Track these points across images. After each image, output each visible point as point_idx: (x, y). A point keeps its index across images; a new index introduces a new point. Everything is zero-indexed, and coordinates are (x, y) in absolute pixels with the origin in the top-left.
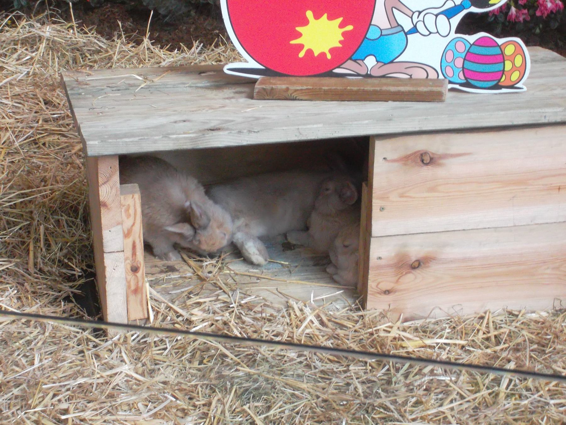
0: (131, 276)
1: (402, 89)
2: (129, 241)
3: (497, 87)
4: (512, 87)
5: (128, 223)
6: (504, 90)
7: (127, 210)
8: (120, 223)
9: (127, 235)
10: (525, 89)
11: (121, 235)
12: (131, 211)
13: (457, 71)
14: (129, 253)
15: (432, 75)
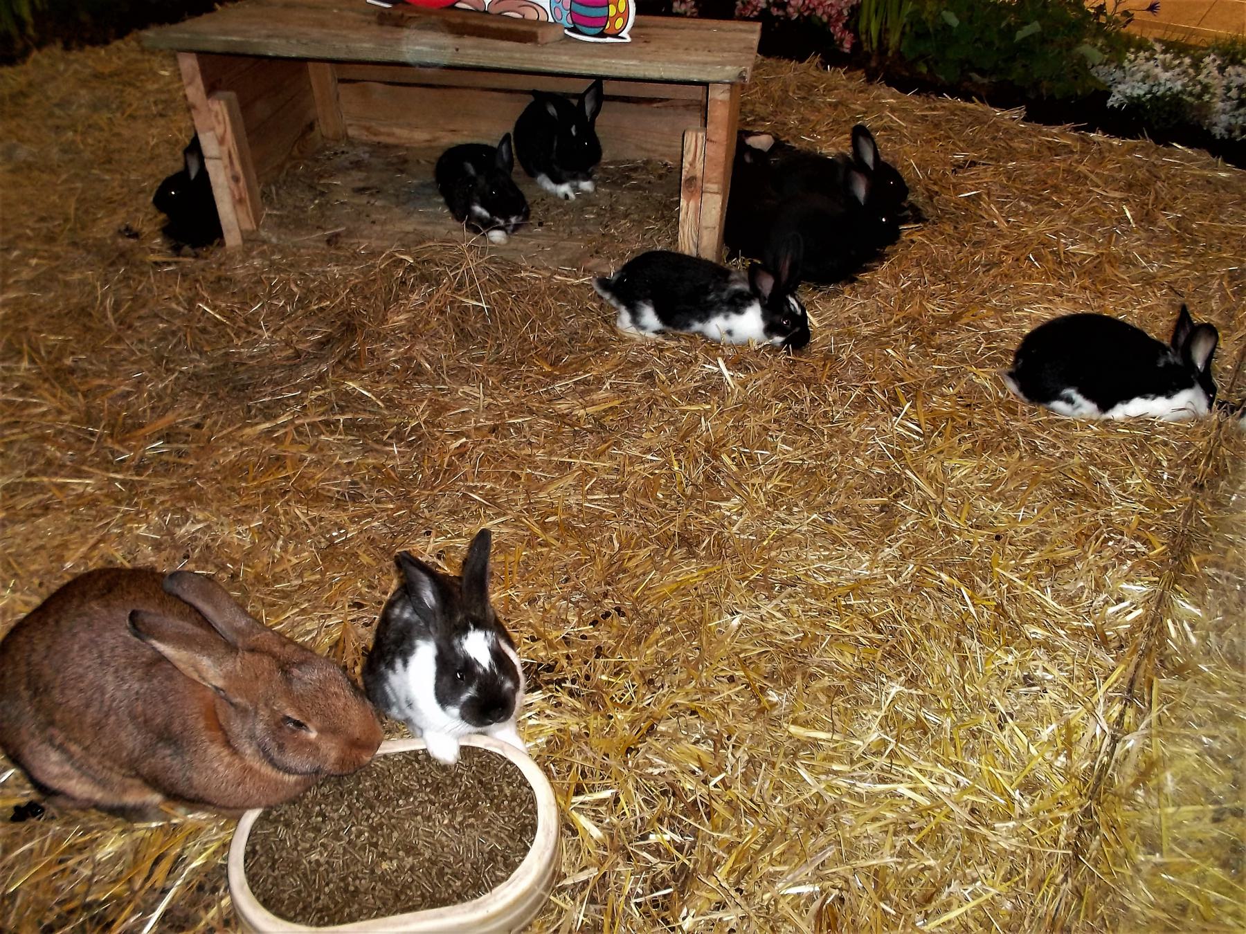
0: (232, 184)
1: (494, 25)
2: (225, 148)
3: (602, 35)
4: (616, 36)
5: (220, 130)
6: (609, 40)
7: (216, 116)
8: (213, 129)
9: (222, 141)
10: (629, 40)
11: (216, 142)
12: (220, 118)
13: (566, 13)
14: (227, 161)
15: (543, 17)
